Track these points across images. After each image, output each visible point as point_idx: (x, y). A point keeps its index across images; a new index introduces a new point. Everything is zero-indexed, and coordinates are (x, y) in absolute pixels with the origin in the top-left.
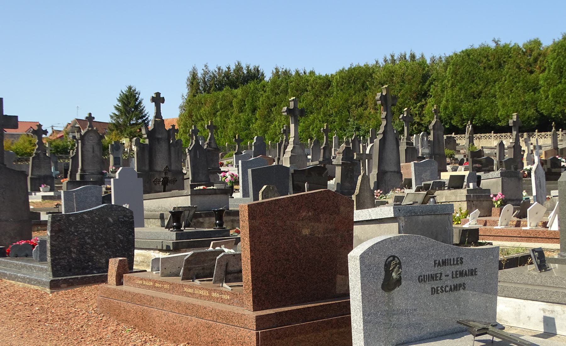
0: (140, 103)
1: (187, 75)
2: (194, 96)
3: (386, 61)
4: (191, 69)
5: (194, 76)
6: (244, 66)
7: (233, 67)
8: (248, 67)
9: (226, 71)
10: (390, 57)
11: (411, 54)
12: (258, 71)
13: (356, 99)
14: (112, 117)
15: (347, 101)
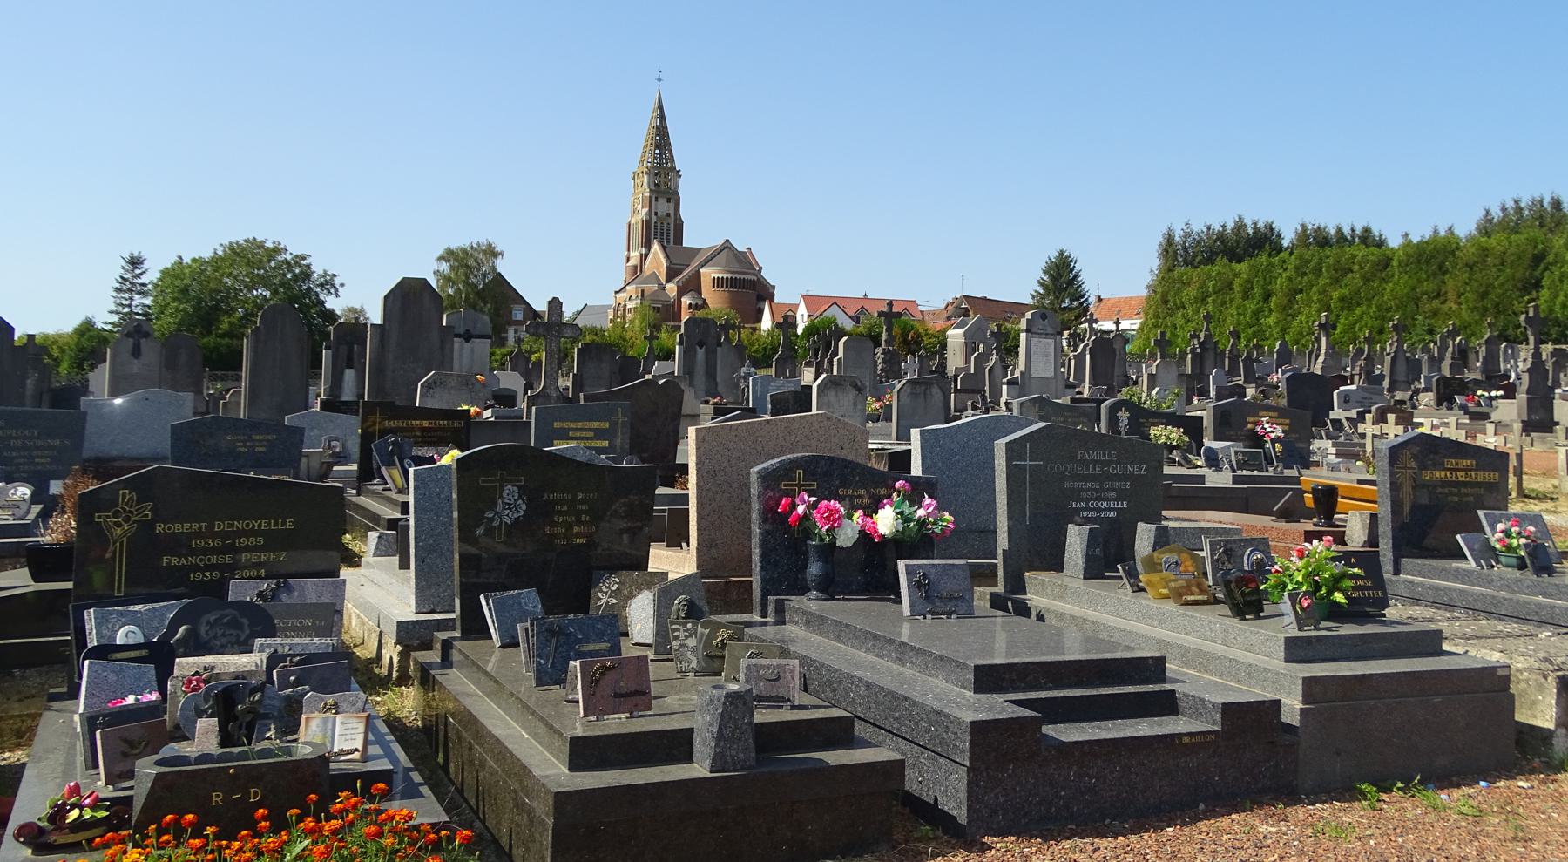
0: (1076, 276)
1: (1158, 239)
2: (1170, 270)
3: (1504, 209)
4: (1165, 230)
5: (1169, 240)
6: (1248, 221)
7: (1230, 225)
8: (1255, 224)
9: (1219, 231)
11: (1552, 198)
12: (1272, 229)
14: (1033, 297)
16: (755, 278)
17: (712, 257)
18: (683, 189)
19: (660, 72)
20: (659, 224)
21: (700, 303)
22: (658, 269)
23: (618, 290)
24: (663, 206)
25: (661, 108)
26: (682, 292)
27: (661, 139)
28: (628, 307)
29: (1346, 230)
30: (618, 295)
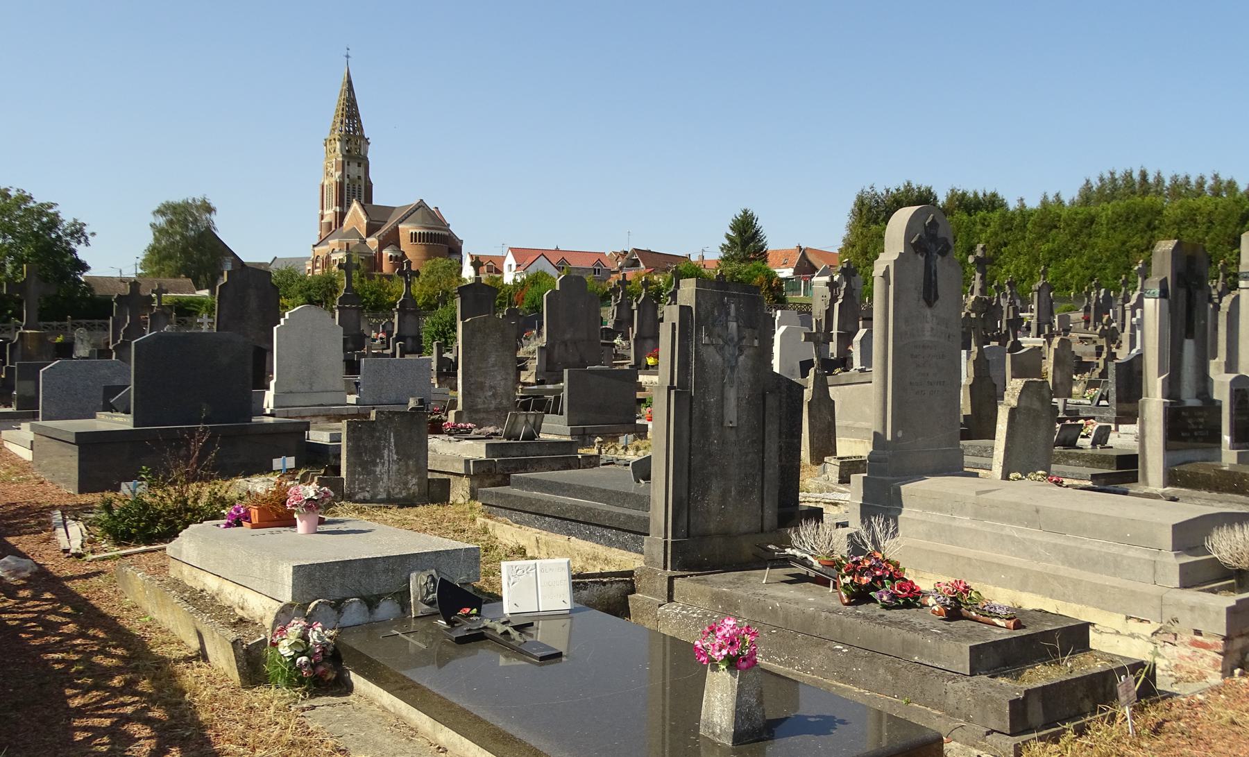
3: (1101, 179)
10: (1109, 175)
11: (1142, 171)
13: (1136, 240)
15: (1124, 243)
16: (447, 233)
17: (409, 214)
18: (372, 155)
19: (348, 49)
20: (351, 186)
21: (400, 255)
22: (357, 225)
23: (315, 244)
24: (354, 170)
25: (350, 82)
26: (382, 245)
27: (350, 110)
28: (333, 258)
29: (981, 195)
30: (316, 249)
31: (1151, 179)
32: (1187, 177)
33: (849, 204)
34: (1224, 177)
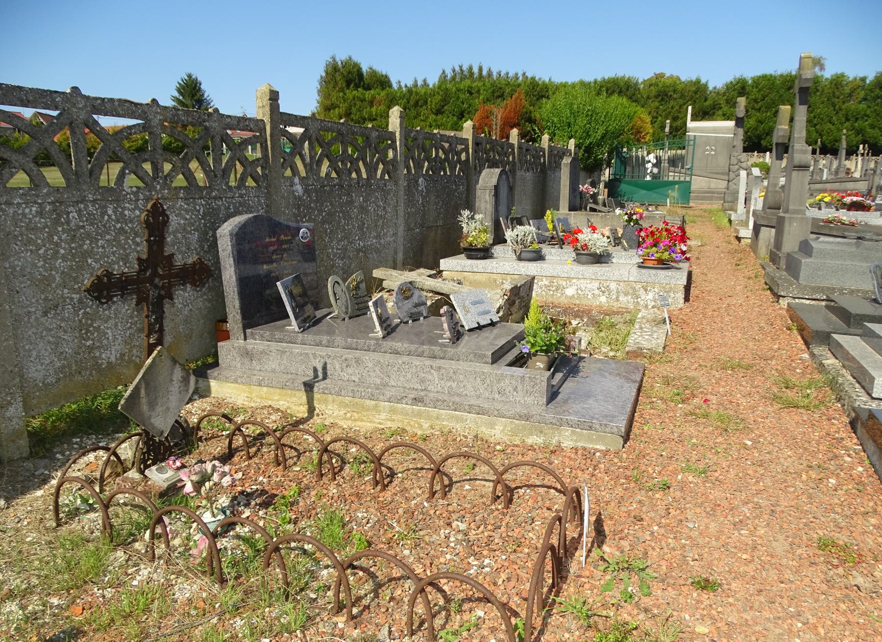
3: (454, 71)
31: (485, 73)
32: (507, 74)
33: (320, 71)
34: (529, 75)
